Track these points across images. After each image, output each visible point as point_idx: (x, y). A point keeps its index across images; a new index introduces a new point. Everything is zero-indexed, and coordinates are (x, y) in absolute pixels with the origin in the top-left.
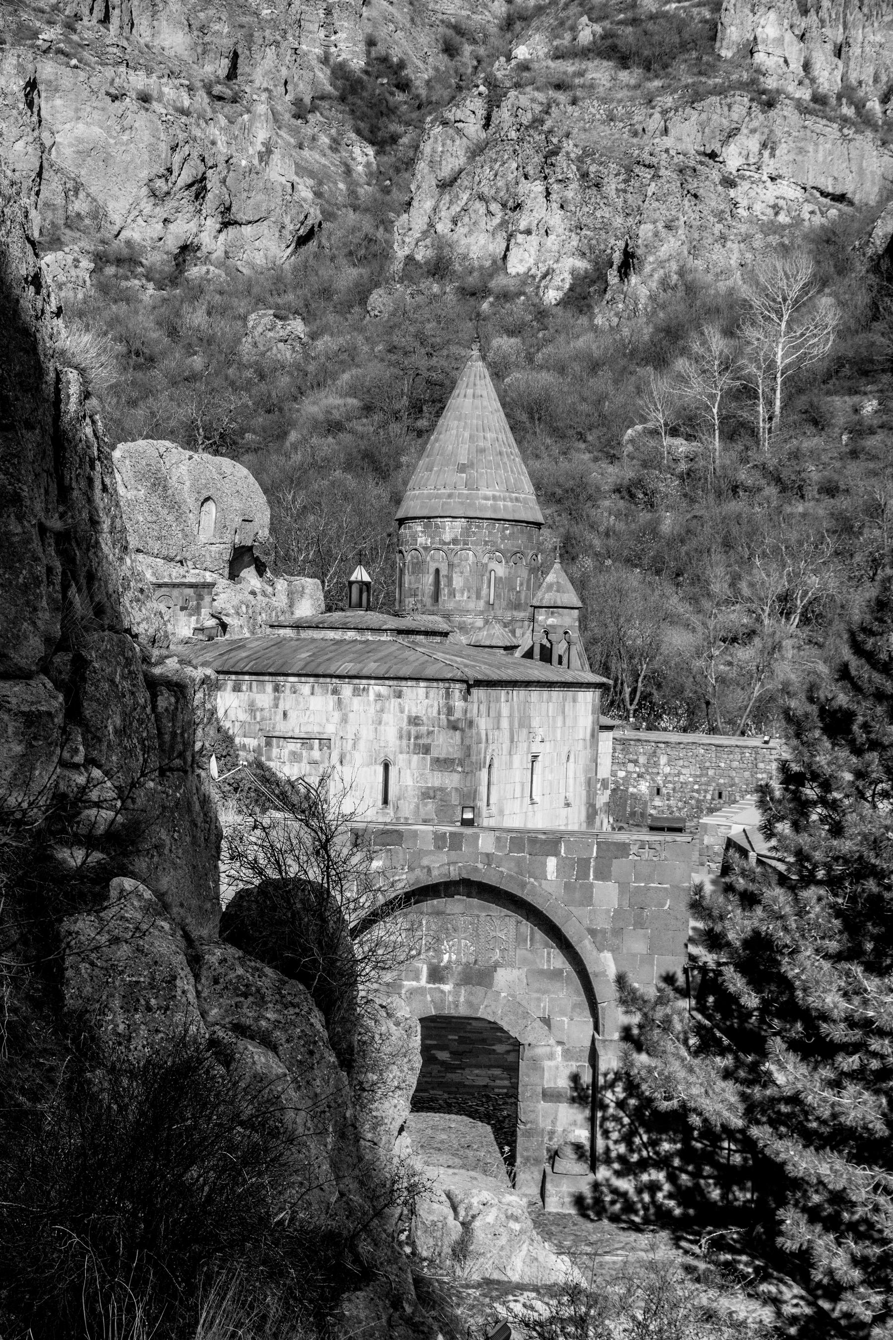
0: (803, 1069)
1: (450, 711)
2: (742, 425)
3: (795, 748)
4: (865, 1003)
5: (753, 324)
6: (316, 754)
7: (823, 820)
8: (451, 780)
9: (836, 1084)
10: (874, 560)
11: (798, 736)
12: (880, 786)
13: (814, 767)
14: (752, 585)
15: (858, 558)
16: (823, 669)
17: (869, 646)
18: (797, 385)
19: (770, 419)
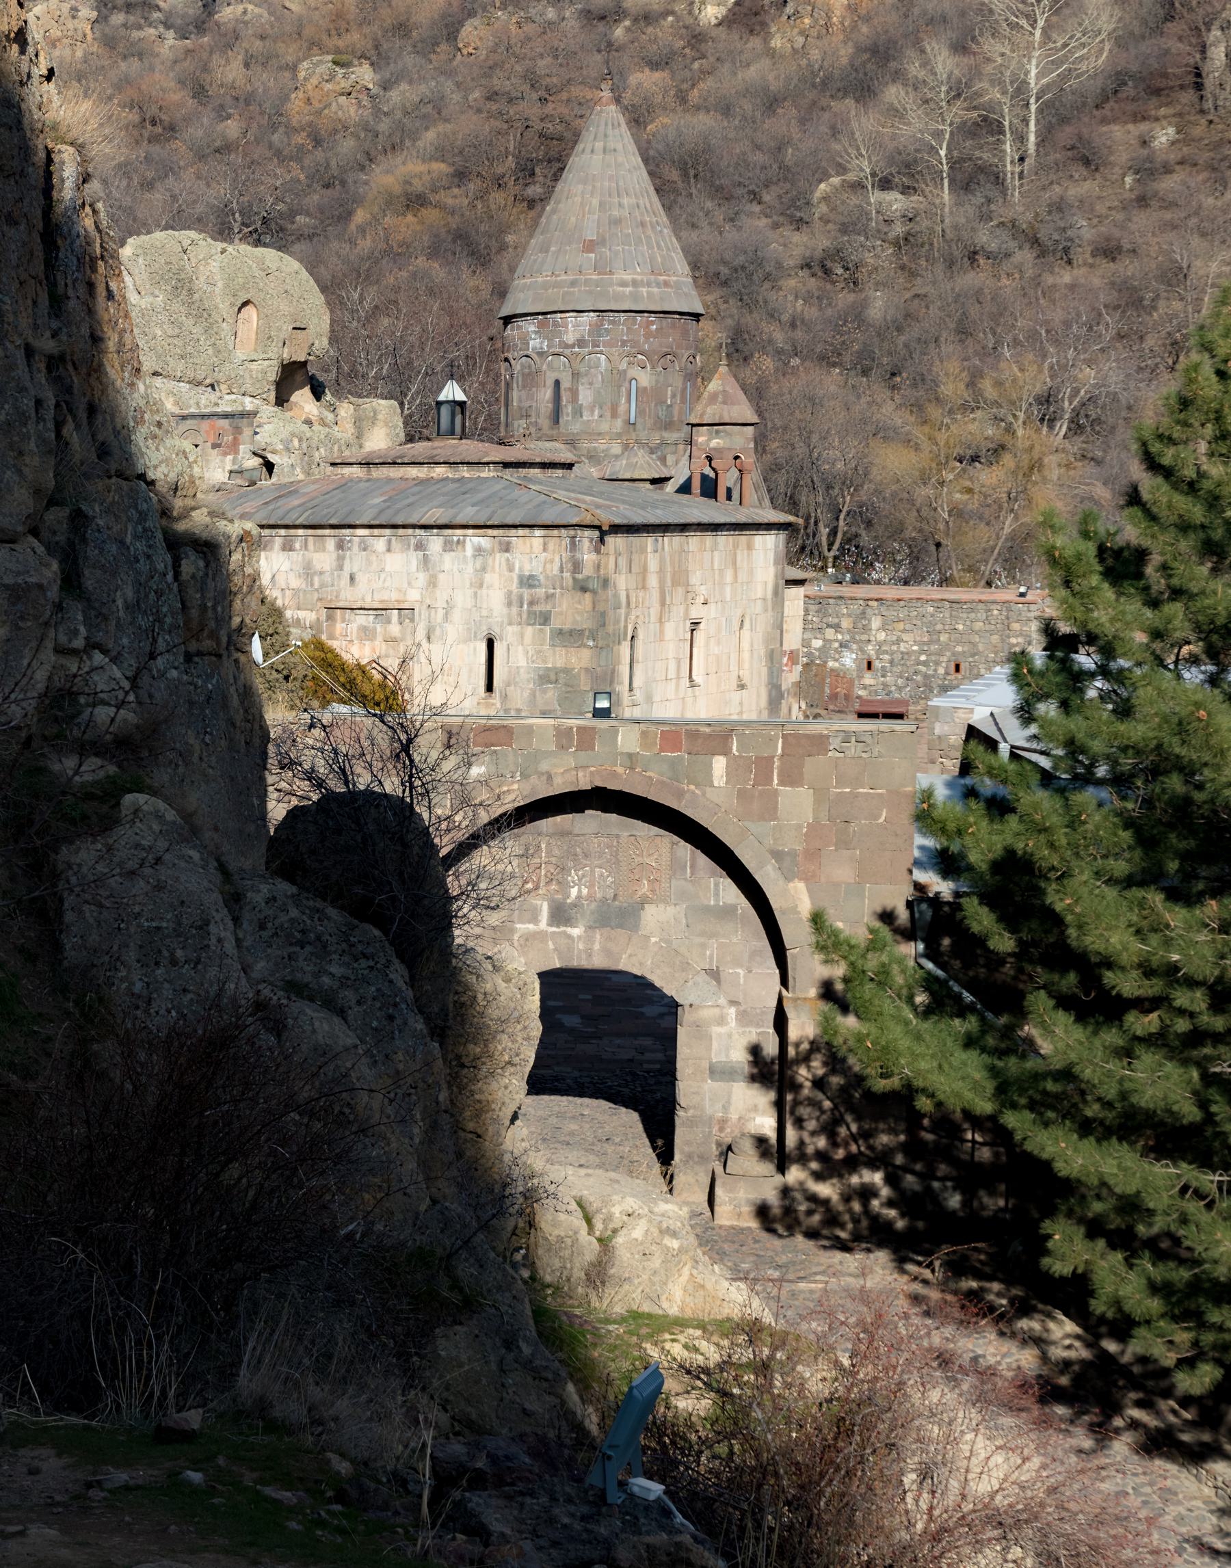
0: (1079, 1033)
1: (577, 566)
2: (981, 169)
3: (1064, 601)
4: (1167, 943)
5: (995, 34)
6: (395, 629)
7: (1103, 697)
8: (579, 659)
9: (1126, 1053)
10: (1175, 343)
11: (1067, 584)
12: (1185, 650)
13: (1091, 626)
14: (998, 384)
15: (1150, 341)
16: (1103, 493)
17: (1166, 461)
18: (1057, 113)
19: (1022, 159)
